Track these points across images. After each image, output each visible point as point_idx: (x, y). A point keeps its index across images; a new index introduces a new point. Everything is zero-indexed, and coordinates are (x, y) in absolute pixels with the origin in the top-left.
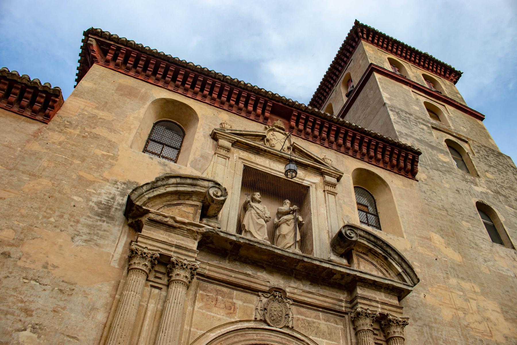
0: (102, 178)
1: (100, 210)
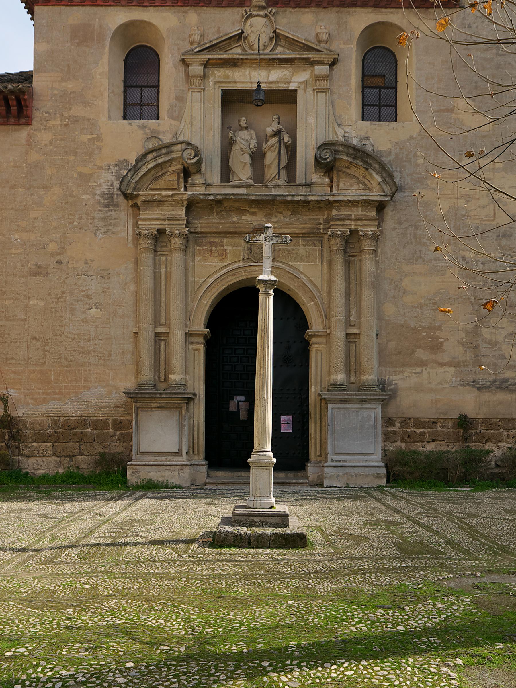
0: (96, 167)
1: (106, 201)
